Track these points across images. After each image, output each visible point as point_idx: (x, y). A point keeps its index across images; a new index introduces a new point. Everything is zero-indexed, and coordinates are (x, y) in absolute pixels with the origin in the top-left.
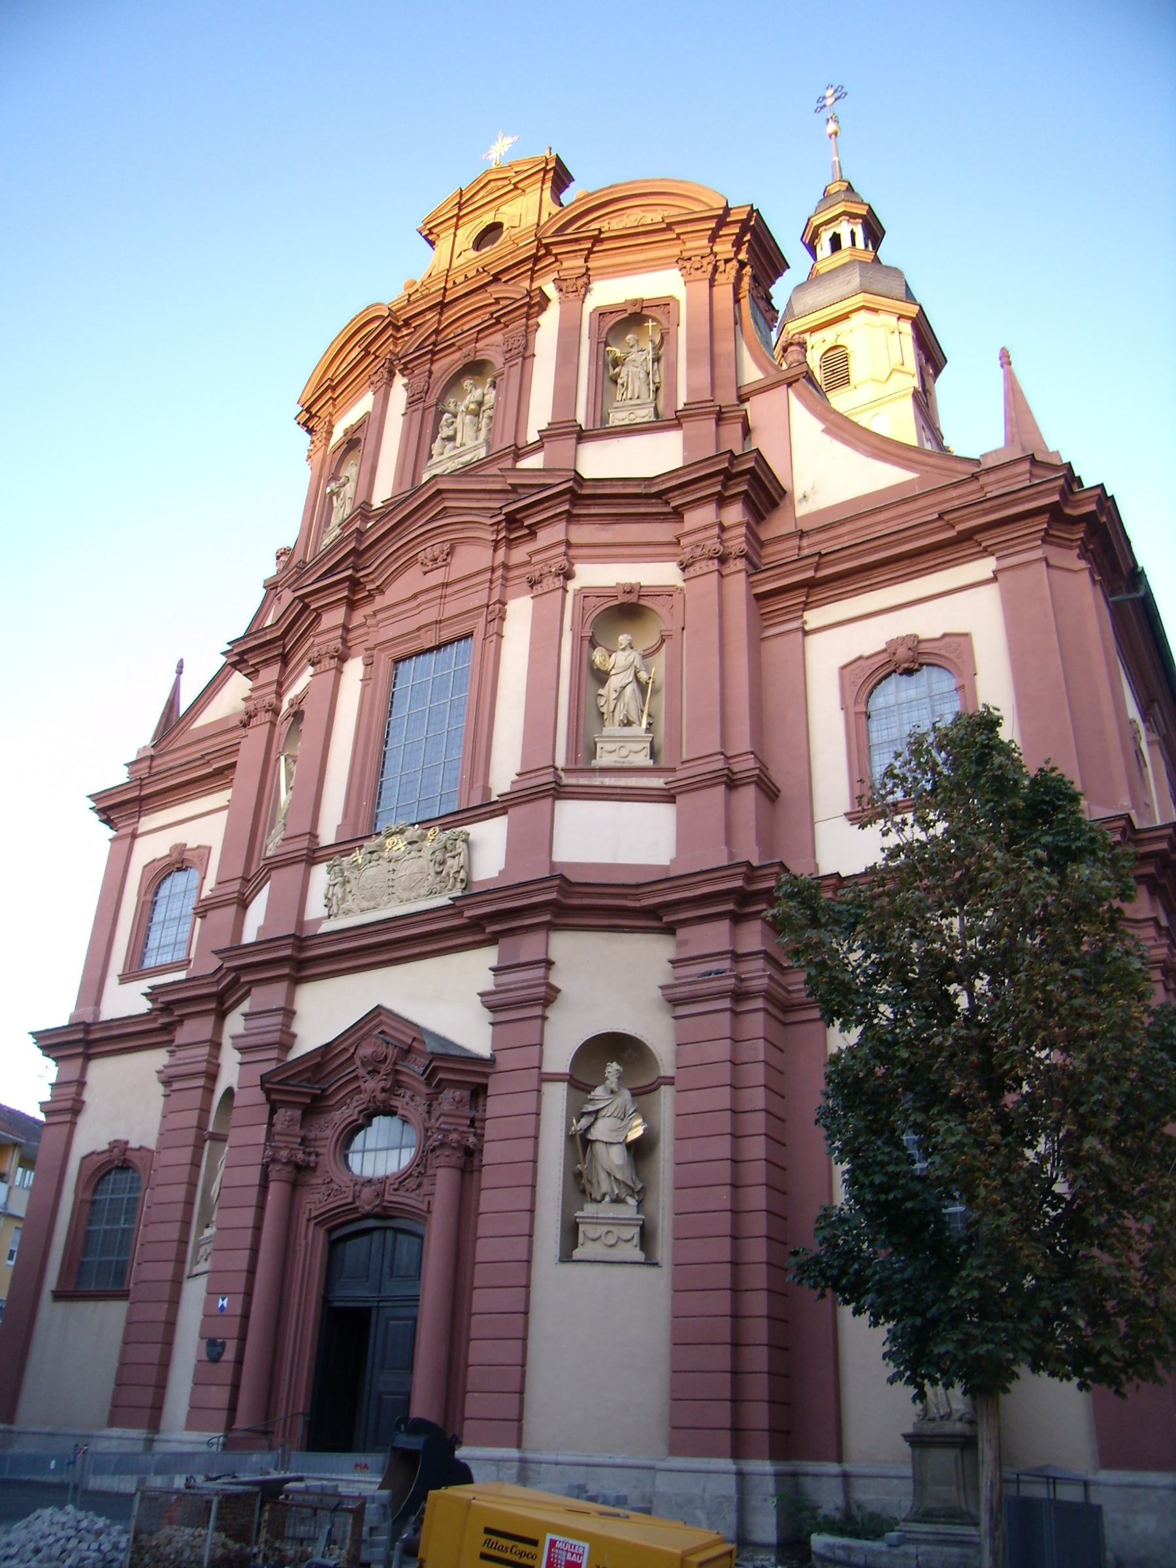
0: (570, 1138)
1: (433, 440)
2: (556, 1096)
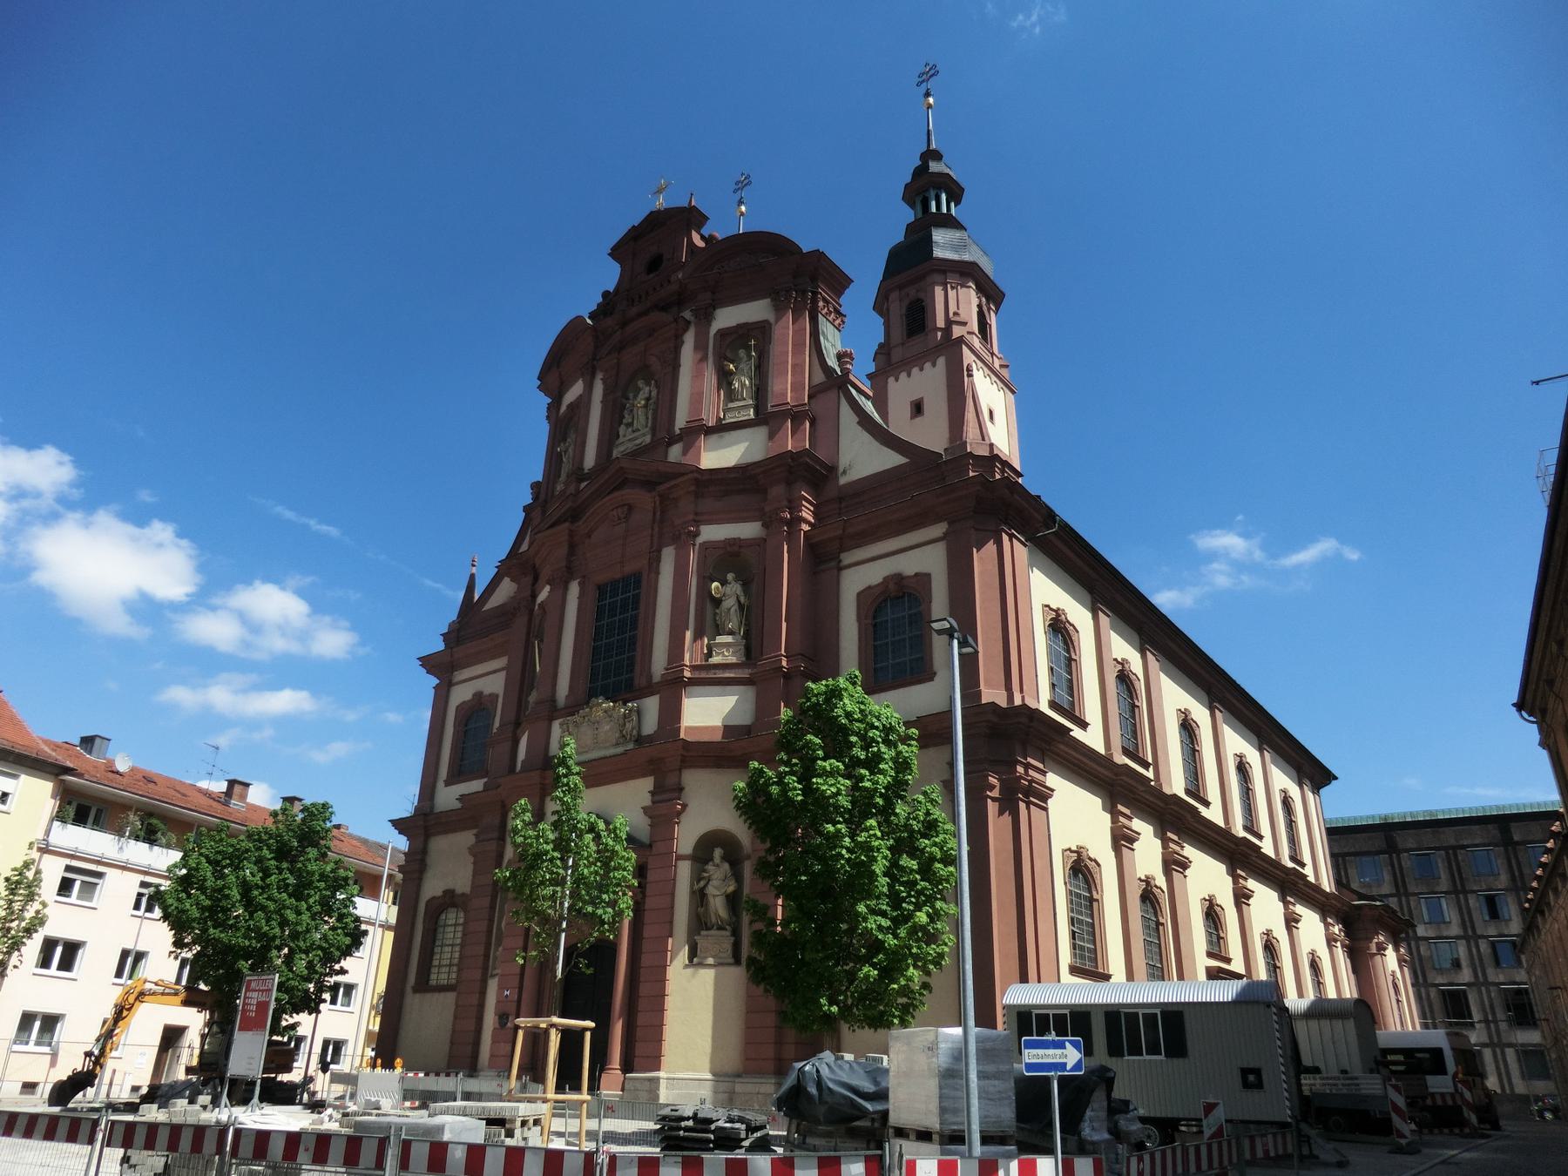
0: (693, 893)
1: (621, 423)
2: (684, 870)
